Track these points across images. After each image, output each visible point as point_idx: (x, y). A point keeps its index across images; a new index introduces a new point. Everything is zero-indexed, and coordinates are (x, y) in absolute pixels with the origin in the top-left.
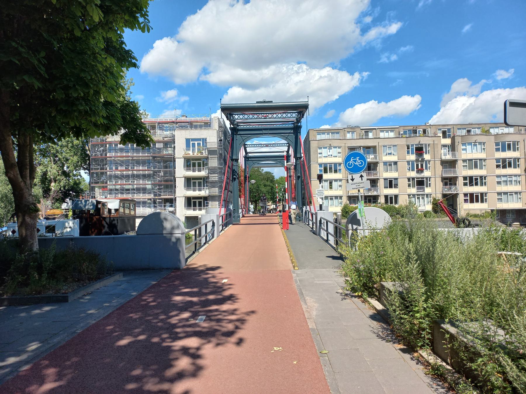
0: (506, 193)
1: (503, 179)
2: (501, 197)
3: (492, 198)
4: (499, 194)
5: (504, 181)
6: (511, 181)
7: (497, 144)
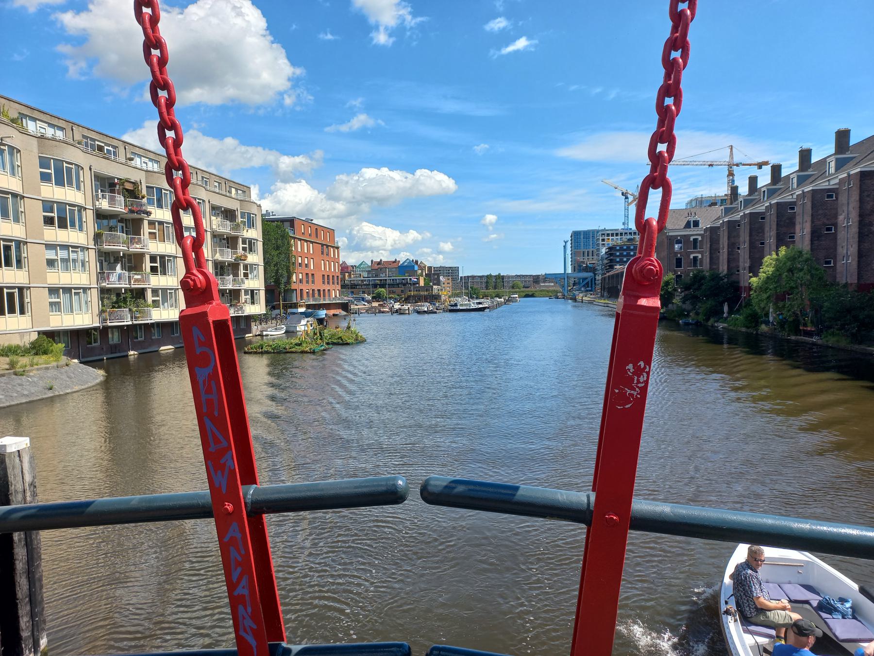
0: (67, 290)
1: (62, 254)
2: (58, 300)
3: (38, 299)
4: (53, 291)
5: (63, 260)
6: (74, 260)
7: (44, 163)
